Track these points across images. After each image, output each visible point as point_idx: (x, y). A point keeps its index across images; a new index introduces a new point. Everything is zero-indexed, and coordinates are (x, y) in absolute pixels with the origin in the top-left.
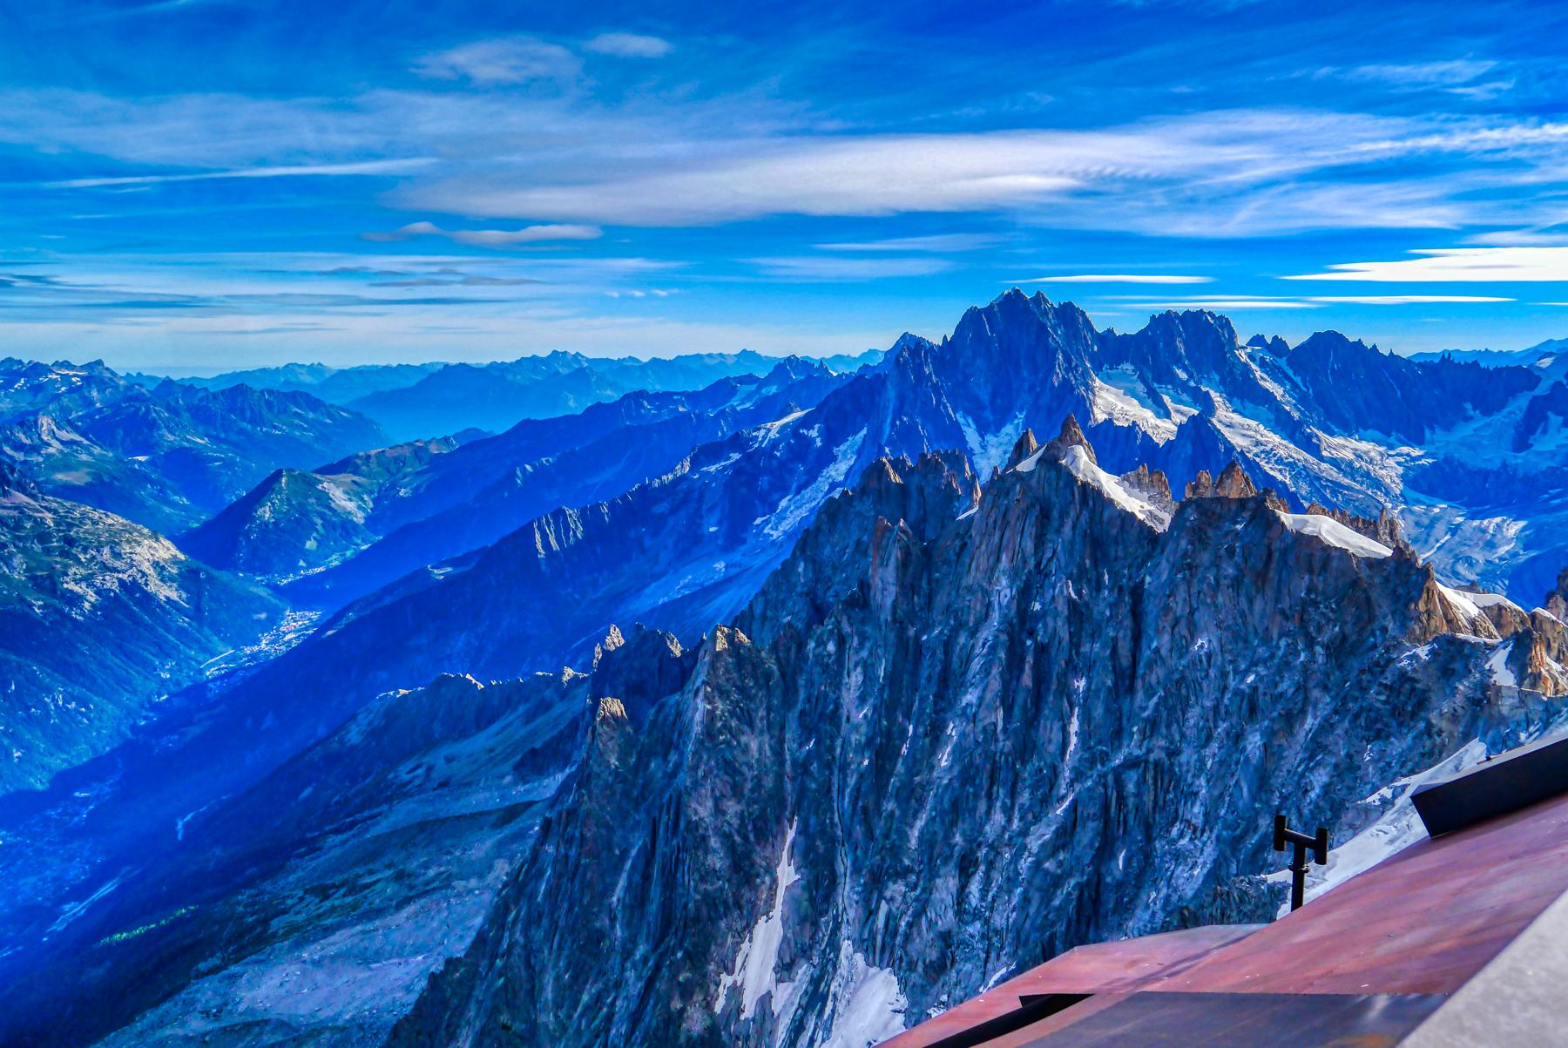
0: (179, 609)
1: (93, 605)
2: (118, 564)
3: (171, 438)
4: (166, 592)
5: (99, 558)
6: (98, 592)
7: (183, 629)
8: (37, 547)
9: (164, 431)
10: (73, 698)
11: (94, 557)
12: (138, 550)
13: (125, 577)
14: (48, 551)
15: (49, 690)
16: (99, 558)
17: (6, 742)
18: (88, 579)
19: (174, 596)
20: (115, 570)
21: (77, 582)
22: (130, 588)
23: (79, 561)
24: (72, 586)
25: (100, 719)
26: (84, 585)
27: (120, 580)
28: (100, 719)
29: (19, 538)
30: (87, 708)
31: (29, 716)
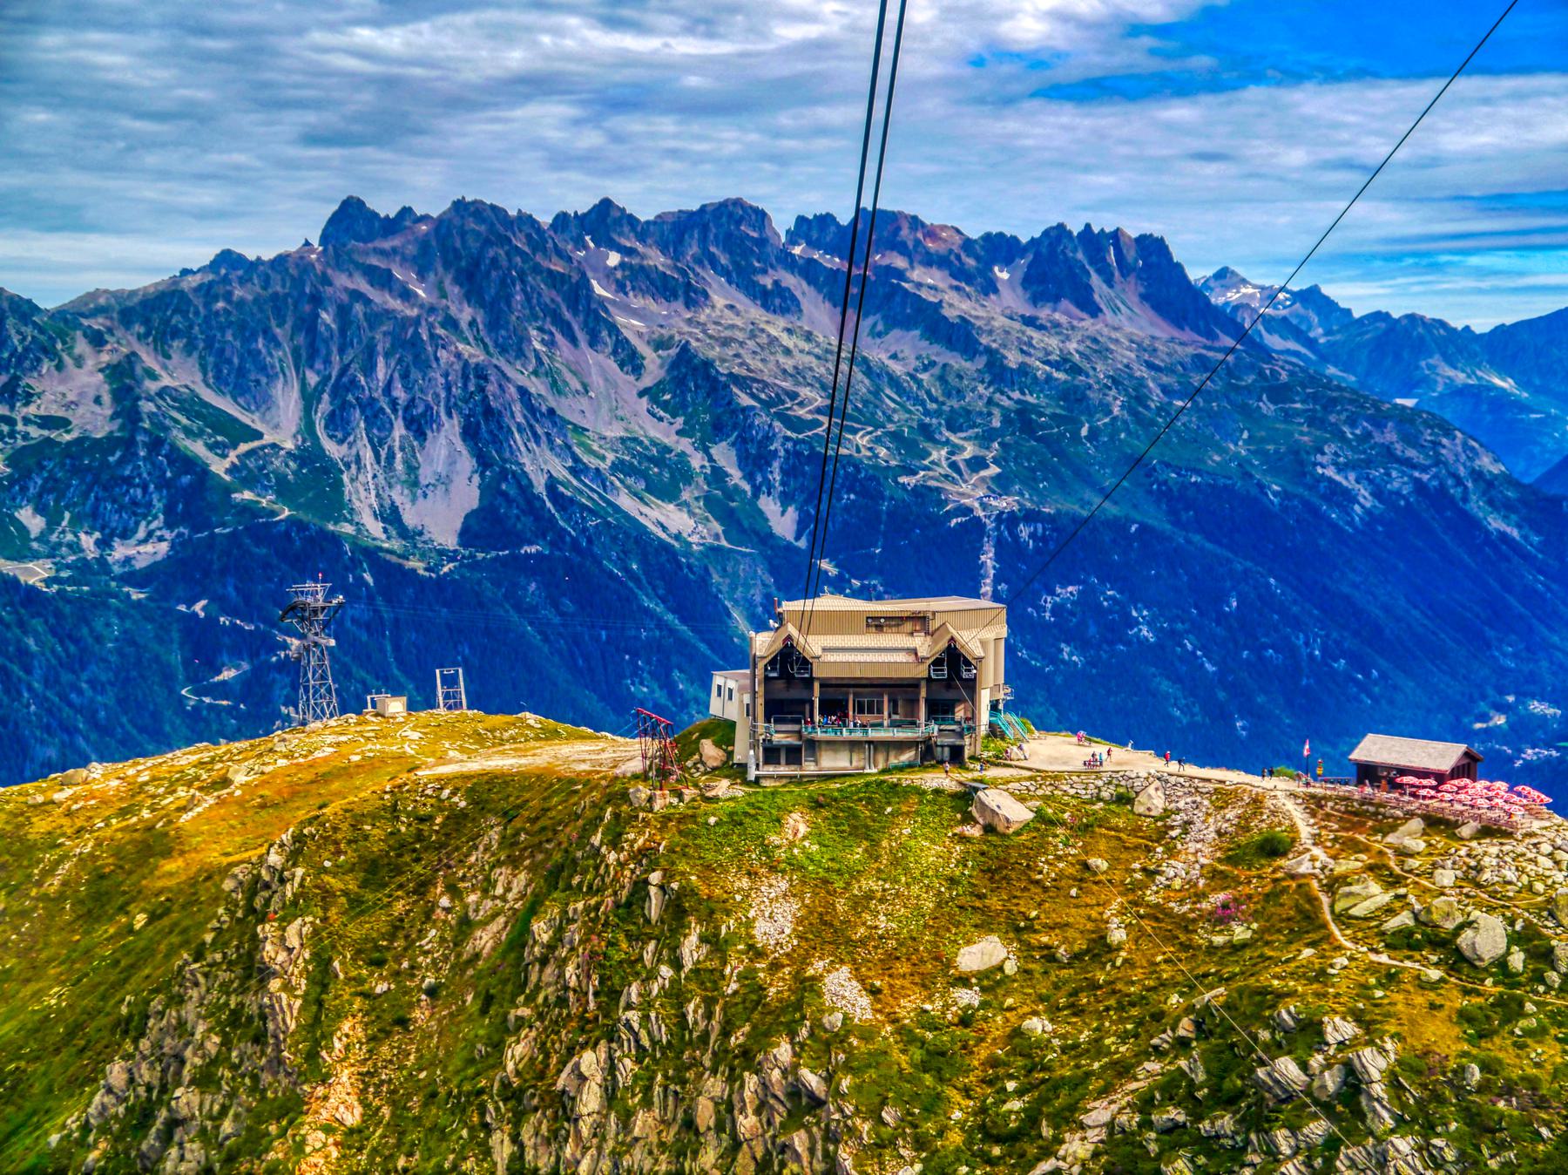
0: (1526, 557)
1: (1368, 512)
2: (1411, 453)
3: (1450, 372)
4: (1495, 523)
5: (1378, 438)
6: (1377, 494)
7: (1536, 591)
8: (1267, 407)
9: (1436, 360)
10: (1343, 654)
11: (1368, 436)
12: (1445, 441)
13: (1425, 477)
14: (1288, 416)
15: (1297, 624)
16: (1378, 438)
17: (1221, 695)
18: (1359, 466)
19: (1515, 533)
20: (1408, 463)
21: (1340, 469)
22: (1437, 498)
23: (1341, 437)
24: (1330, 472)
25: (1391, 702)
26: (1352, 476)
27: (1417, 482)
28: (1391, 702)
29: (1237, 388)
30: (1367, 675)
31: (1261, 658)
